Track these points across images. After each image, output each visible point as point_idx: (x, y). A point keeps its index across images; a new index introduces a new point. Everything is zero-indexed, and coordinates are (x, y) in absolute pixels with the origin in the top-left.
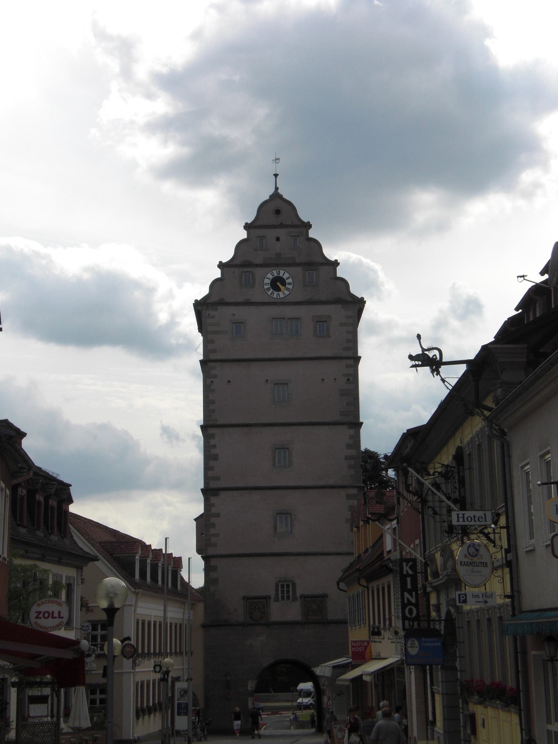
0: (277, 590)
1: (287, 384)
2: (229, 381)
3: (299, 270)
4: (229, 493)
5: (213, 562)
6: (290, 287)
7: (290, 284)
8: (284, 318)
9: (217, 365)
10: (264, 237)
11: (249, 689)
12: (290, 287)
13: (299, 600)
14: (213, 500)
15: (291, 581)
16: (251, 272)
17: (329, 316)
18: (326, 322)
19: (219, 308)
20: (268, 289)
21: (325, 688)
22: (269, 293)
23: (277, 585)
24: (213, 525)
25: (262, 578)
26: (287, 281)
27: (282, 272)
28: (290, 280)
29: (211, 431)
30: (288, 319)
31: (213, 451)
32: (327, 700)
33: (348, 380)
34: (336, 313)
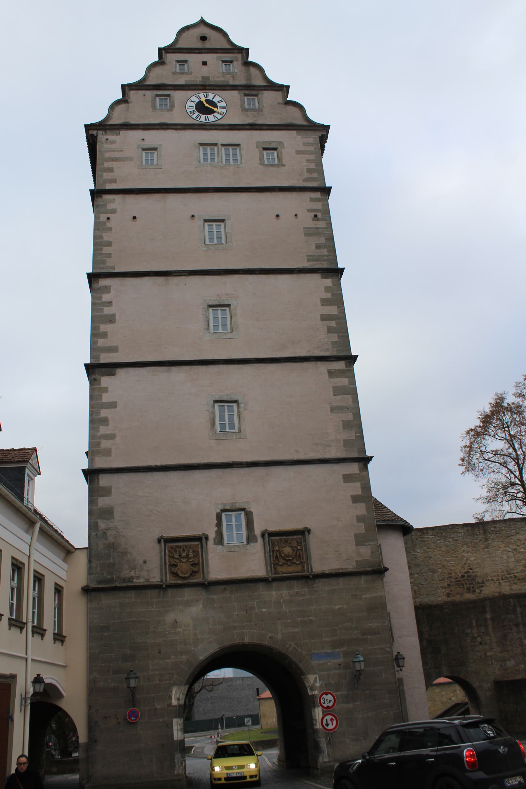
0: (219, 525)
1: (223, 221)
2: (134, 218)
3: (235, 94)
4: (132, 371)
5: (104, 480)
8: (216, 145)
9: (118, 198)
10: (186, 62)
11: (174, 702)
13: (260, 540)
14: (105, 381)
15: (244, 510)
16: (169, 95)
17: (281, 143)
18: (275, 149)
19: (122, 132)
20: (193, 113)
21: (316, 692)
22: (194, 116)
23: (219, 517)
24: (105, 421)
25: (192, 504)
28: (223, 104)
29: (104, 282)
30: (223, 145)
31: (107, 311)
32: (321, 716)
33: (316, 216)
34: (290, 141)
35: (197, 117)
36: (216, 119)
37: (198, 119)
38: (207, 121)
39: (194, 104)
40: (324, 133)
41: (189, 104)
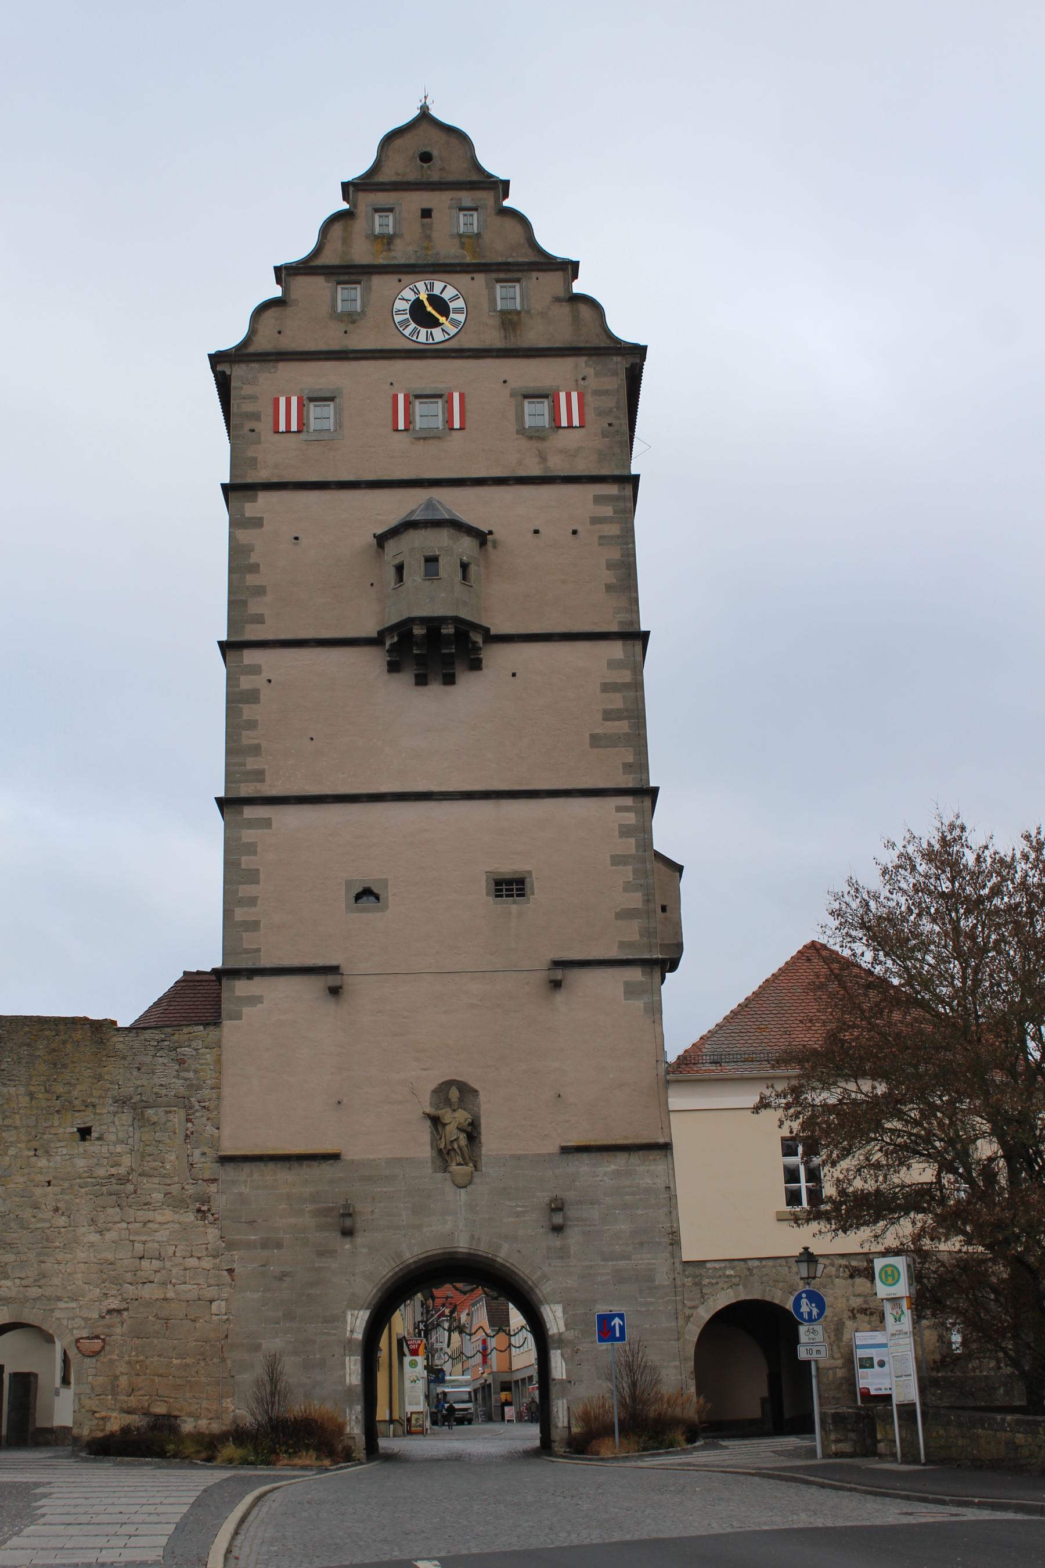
6: (461, 318)
7: (458, 311)
12: (461, 318)
20: (405, 323)
26: (452, 305)
27: (438, 287)
28: (460, 303)
35: (412, 334)
36: (447, 337)
37: (414, 338)
38: (431, 341)
39: (407, 306)
40: (638, 361)
41: (399, 305)
